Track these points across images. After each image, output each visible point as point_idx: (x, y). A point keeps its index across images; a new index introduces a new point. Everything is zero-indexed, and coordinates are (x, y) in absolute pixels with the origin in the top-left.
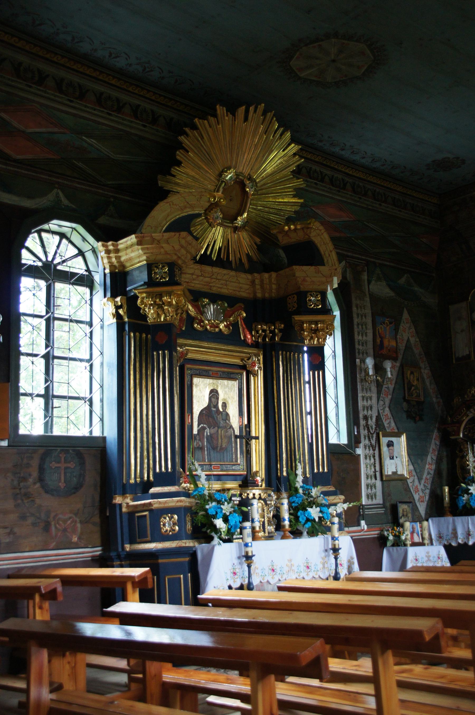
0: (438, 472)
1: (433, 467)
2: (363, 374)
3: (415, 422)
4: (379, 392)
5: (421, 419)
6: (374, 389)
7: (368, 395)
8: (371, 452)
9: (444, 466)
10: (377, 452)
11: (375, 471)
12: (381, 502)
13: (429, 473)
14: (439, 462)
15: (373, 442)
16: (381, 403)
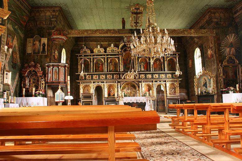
0: (17, 85)
1: (16, 83)
2: (2, 51)
3: (14, 69)
4: (6, 58)
5: (15, 69)
6: (5, 56)
7: (3, 58)
8: (1, 75)
9: (19, 83)
10: (3, 76)
11: (2, 82)
12: (2, 91)
13: (15, 85)
14: (18, 81)
15: (2, 73)
16: (6, 61)
